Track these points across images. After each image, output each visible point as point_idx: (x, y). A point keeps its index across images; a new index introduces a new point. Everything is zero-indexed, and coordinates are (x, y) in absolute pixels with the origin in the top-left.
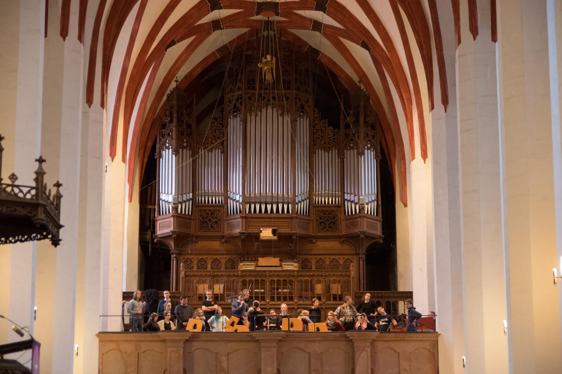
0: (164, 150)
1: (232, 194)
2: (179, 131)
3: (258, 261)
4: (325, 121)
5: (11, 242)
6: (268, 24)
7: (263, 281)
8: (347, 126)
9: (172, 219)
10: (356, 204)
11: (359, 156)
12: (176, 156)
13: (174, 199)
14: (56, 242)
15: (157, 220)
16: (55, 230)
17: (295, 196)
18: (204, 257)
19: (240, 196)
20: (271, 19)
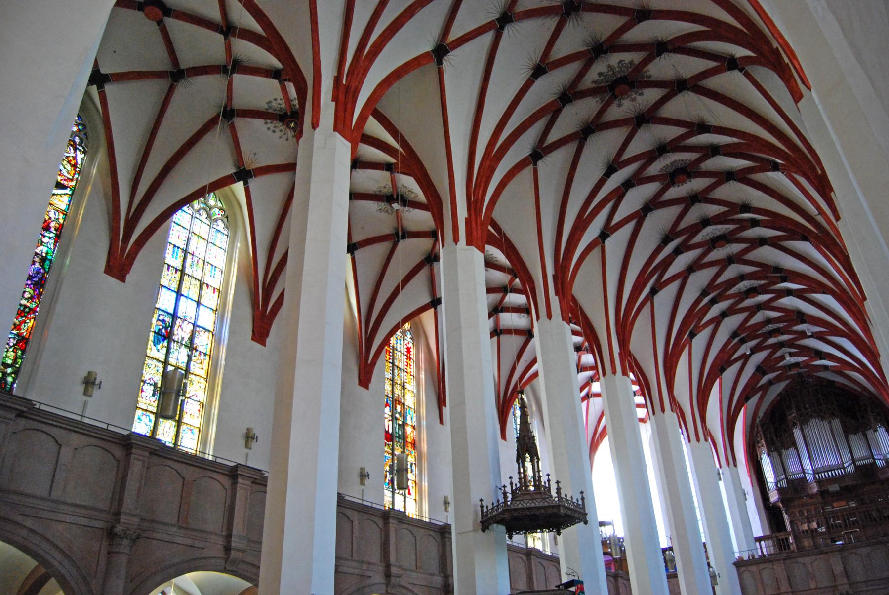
7: (837, 516)
9: (776, 491)
10: (882, 460)
14: (586, 523)
17: (843, 463)
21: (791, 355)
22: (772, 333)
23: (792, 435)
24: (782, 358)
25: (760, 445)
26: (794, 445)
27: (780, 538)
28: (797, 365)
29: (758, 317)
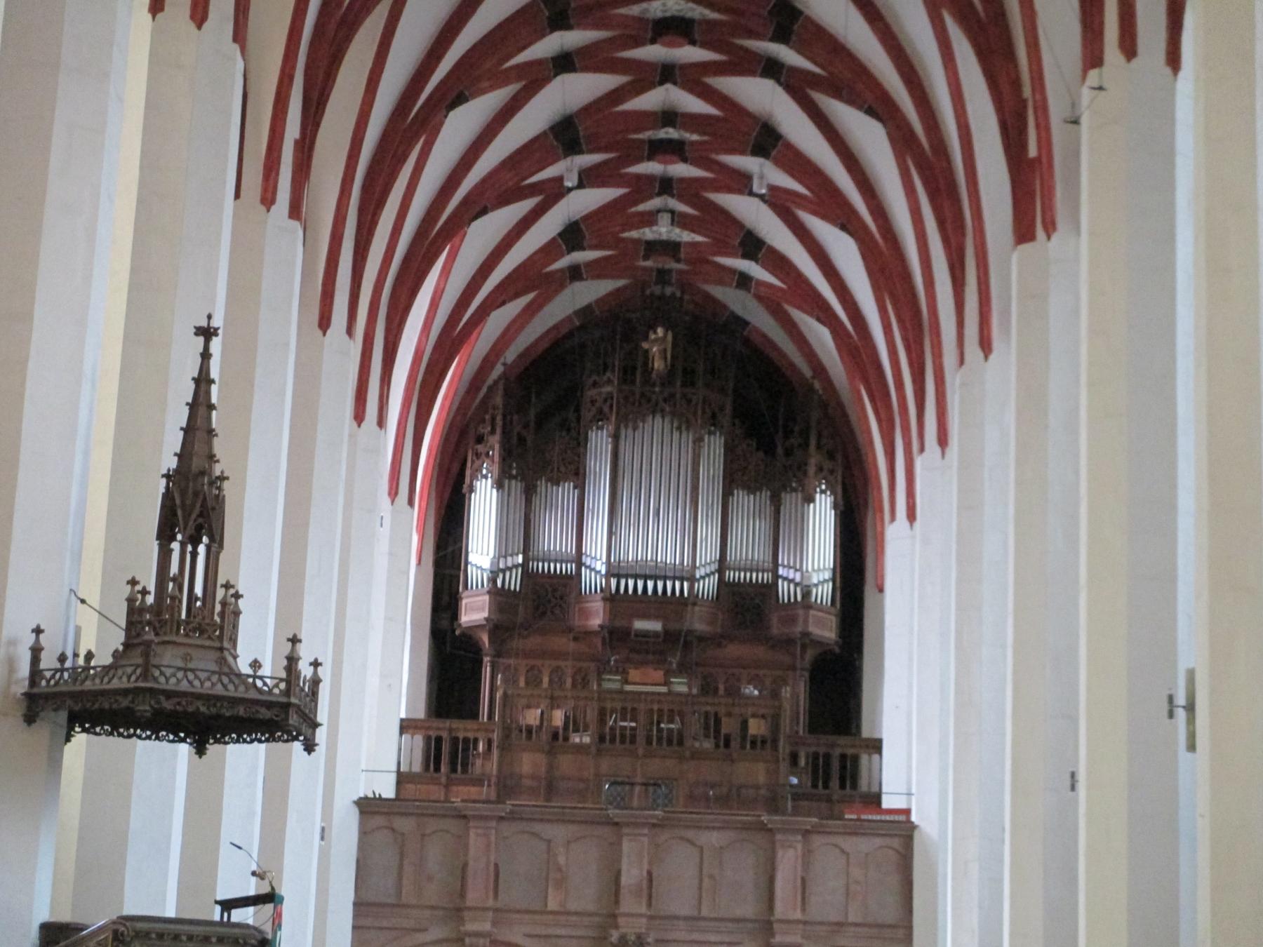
0: (478, 480)
1: (589, 559)
2: (504, 450)
3: (628, 673)
4: (751, 442)
5: (245, 741)
6: (663, 276)
7: (634, 709)
8: (788, 453)
9: (487, 598)
10: (796, 585)
11: (806, 505)
12: (498, 491)
13: (492, 564)
14: (310, 747)
15: (461, 599)
16: (310, 731)
17: (694, 567)
18: (538, 662)
19: (603, 563)
20: (667, 267)
21: (678, 220)
22: (658, 149)
23: (578, 447)
24: (649, 219)
25: (480, 448)
26: (578, 475)
27: (461, 735)
28: (671, 248)
29: (651, 100)
